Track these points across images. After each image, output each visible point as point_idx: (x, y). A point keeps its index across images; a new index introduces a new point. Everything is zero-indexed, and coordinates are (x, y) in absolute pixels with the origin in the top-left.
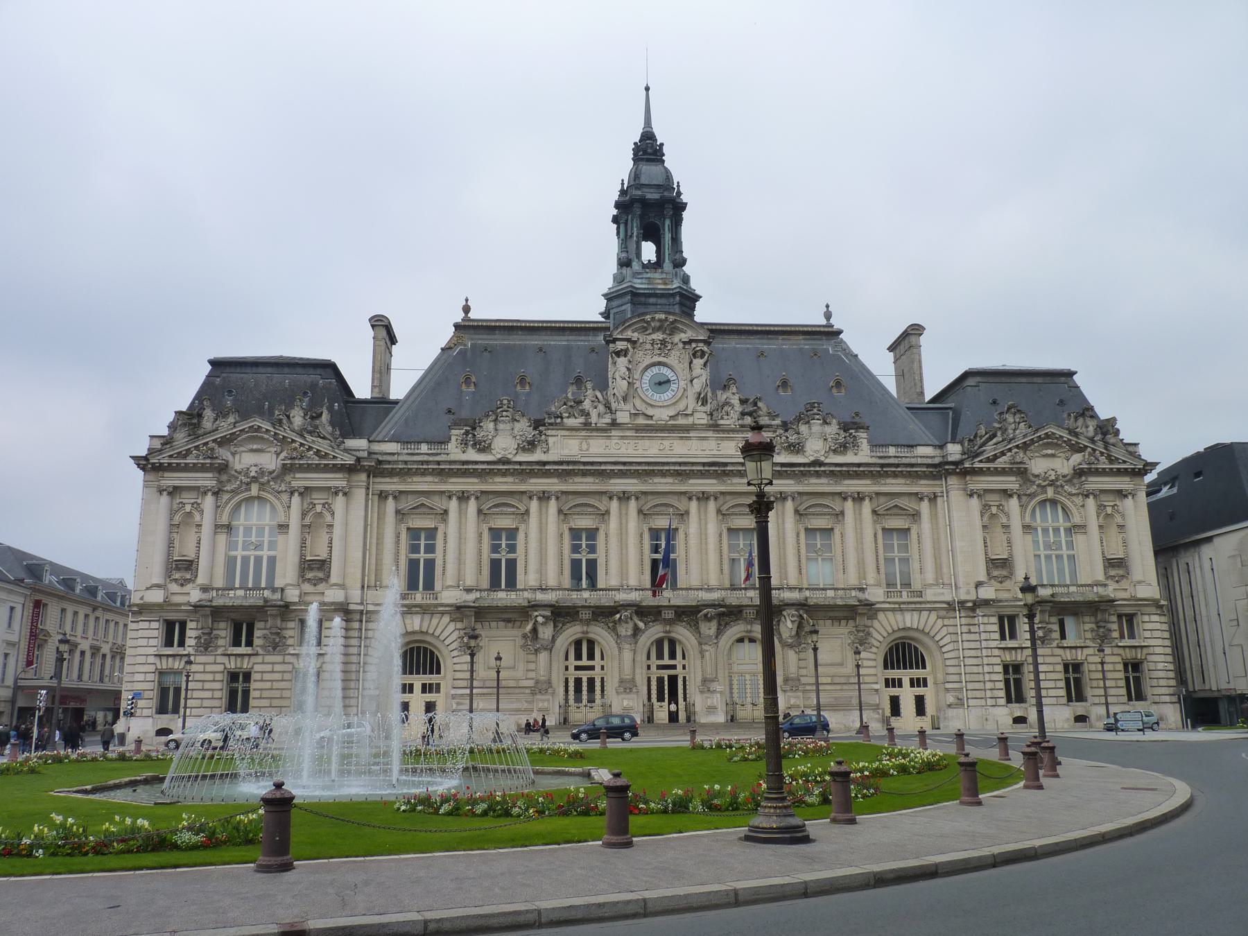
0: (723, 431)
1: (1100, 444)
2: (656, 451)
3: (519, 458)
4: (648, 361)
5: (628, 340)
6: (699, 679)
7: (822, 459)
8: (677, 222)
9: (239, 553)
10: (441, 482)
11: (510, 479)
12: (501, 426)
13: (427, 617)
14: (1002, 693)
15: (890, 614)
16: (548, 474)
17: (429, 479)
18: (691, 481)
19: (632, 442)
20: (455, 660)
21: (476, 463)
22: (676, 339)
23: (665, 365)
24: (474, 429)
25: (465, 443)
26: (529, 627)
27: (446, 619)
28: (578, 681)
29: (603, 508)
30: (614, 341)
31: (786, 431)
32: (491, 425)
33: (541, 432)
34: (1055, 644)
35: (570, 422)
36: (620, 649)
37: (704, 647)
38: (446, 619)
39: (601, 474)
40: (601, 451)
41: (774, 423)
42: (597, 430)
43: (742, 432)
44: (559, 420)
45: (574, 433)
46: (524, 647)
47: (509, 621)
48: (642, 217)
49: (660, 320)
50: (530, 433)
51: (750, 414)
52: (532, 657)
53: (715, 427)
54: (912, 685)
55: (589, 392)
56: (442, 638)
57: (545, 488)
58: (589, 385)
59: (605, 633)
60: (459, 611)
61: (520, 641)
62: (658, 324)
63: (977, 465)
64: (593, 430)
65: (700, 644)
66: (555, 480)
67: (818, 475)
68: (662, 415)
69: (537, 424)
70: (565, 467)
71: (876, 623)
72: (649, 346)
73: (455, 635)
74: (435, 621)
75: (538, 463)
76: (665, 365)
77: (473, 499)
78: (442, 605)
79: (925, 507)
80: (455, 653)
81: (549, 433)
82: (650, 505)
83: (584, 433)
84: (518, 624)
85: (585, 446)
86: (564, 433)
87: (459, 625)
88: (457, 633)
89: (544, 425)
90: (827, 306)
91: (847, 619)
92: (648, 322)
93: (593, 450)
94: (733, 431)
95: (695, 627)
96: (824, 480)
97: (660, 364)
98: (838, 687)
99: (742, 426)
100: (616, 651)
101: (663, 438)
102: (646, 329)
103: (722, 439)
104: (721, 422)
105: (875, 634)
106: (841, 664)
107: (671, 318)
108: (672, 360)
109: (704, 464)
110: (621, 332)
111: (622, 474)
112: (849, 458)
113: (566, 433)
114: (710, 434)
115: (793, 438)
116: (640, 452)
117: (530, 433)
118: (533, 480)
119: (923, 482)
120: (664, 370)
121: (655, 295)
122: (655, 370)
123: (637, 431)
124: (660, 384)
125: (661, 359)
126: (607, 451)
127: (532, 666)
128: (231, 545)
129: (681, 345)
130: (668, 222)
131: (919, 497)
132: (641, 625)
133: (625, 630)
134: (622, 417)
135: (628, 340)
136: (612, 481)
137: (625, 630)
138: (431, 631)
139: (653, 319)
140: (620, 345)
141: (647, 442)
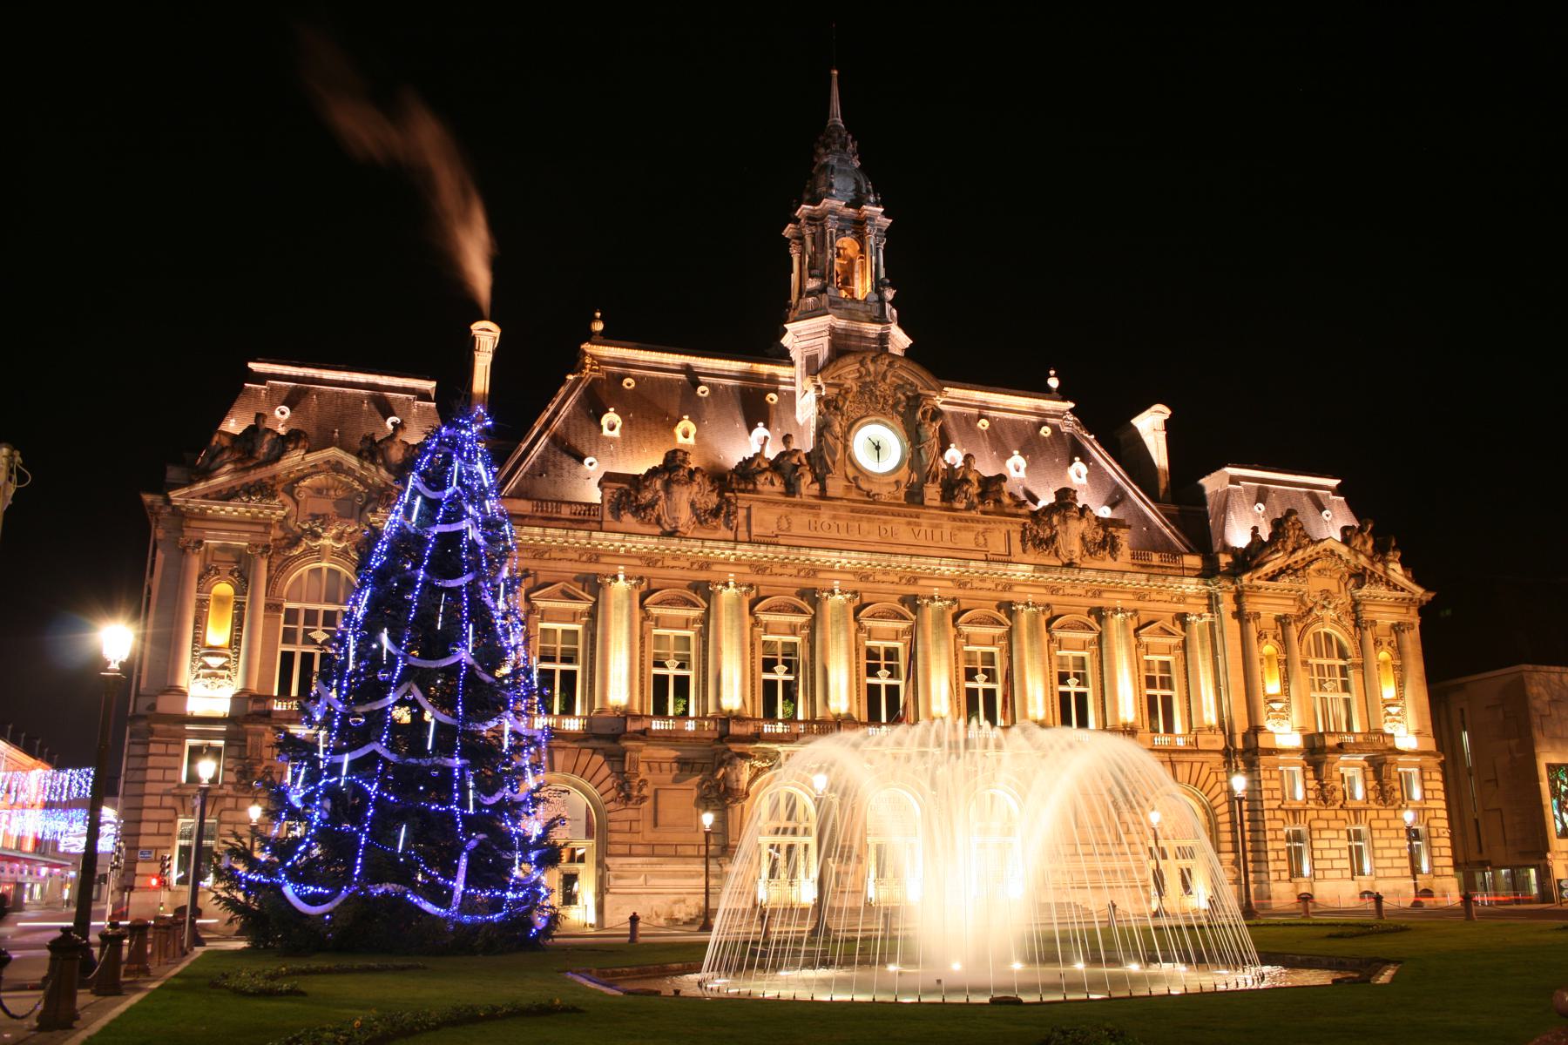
1: (1379, 566)
2: (877, 539)
7: (1077, 561)
9: (298, 649)
14: (1285, 865)
33: (728, 500)
34: (1337, 806)
40: (806, 532)
50: (713, 500)
63: (1257, 582)
64: (795, 505)
85: (784, 525)
93: (794, 531)
103: (959, 529)
115: (1045, 533)
116: (857, 537)
117: (713, 500)
126: (814, 534)
128: (289, 637)
141: (865, 526)
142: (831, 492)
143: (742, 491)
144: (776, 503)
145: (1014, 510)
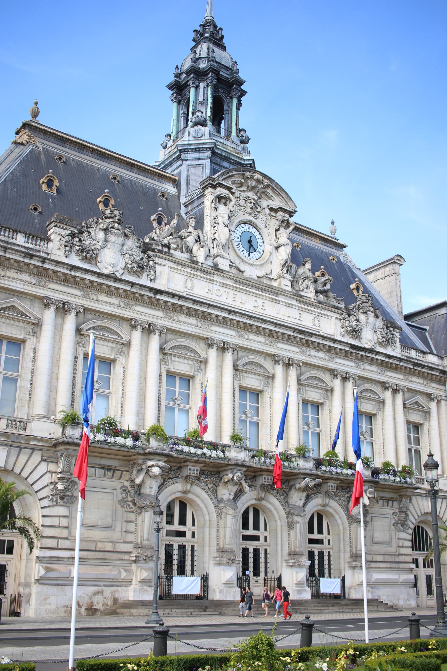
0: (304, 303)
3: (123, 278)
4: (241, 217)
5: (229, 189)
6: (286, 552)
8: (239, 105)
10: (39, 285)
11: (114, 300)
12: (112, 238)
13: (14, 451)
15: (419, 498)
16: (153, 304)
17: (25, 277)
18: (280, 345)
19: (232, 292)
20: (46, 512)
21: (87, 271)
22: (265, 203)
23: (255, 226)
24: (81, 233)
25: (69, 245)
26: (138, 481)
27: (37, 457)
28: (169, 547)
29: (203, 354)
30: (214, 187)
31: (349, 316)
32: (101, 235)
33: (149, 257)
35: (178, 254)
36: (219, 516)
37: (296, 518)
38: (37, 457)
39: (205, 317)
41: (339, 305)
42: (202, 271)
43: (318, 308)
44: (166, 250)
45: (180, 267)
46: (123, 502)
47: (107, 468)
48: (215, 88)
49: (258, 181)
51: (321, 292)
52: (132, 516)
53: (298, 297)
54: (424, 567)
55: (191, 229)
56: (31, 480)
57: (151, 320)
58: (192, 222)
59: (204, 495)
60: (53, 449)
61: (119, 495)
62: (253, 183)
64: (197, 270)
65: (289, 514)
66: (160, 314)
67: (372, 361)
68: (251, 272)
69: (146, 248)
70: (175, 301)
71: (411, 508)
72: (242, 202)
73: (47, 480)
74: (23, 458)
75: (151, 289)
76: (255, 226)
77: (73, 313)
78: (34, 438)
79: (433, 405)
80: (45, 503)
81: (157, 260)
82: (244, 361)
83: (189, 270)
84: (118, 473)
86: (171, 264)
87: (52, 467)
88: (48, 475)
89: (153, 250)
90: (333, 223)
91: (393, 500)
92: (246, 179)
94: (311, 305)
95: (285, 495)
96: (374, 368)
97: (249, 223)
98: (388, 565)
99: (320, 302)
100: (214, 516)
101: (257, 296)
102: (241, 185)
103: (303, 310)
104: (302, 293)
105: (411, 517)
106: (388, 544)
107: (266, 182)
108: (259, 222)
109: (295, 330)
110: (224, 179)
111: (224, 322)
112: (389, 351)
113: (174, 266)
114: (294, 302)
117: (138, 255)
118: (139, 308)
119: (434, 385)
120: (253, 230)
121: (229, 160)
122: (246, 227)
123: (236, 282)
124: (250, 242)
125: (251, 218)
126: (209, 296)
127: (131, 527)
129: (267, 211)
130: (235, 101)
131: (430, 397)
132: (247, 489)
133: (226, 493)
134: (223, 264)
135: (229, 189)
136: (214, 328)
137: (226, 493)
138: (17, 470)
139: (252, 177)
140: (225, 192)
142: (220, 267)
143: (161, 252)
144: (183, 265)
145: (336, 304)
